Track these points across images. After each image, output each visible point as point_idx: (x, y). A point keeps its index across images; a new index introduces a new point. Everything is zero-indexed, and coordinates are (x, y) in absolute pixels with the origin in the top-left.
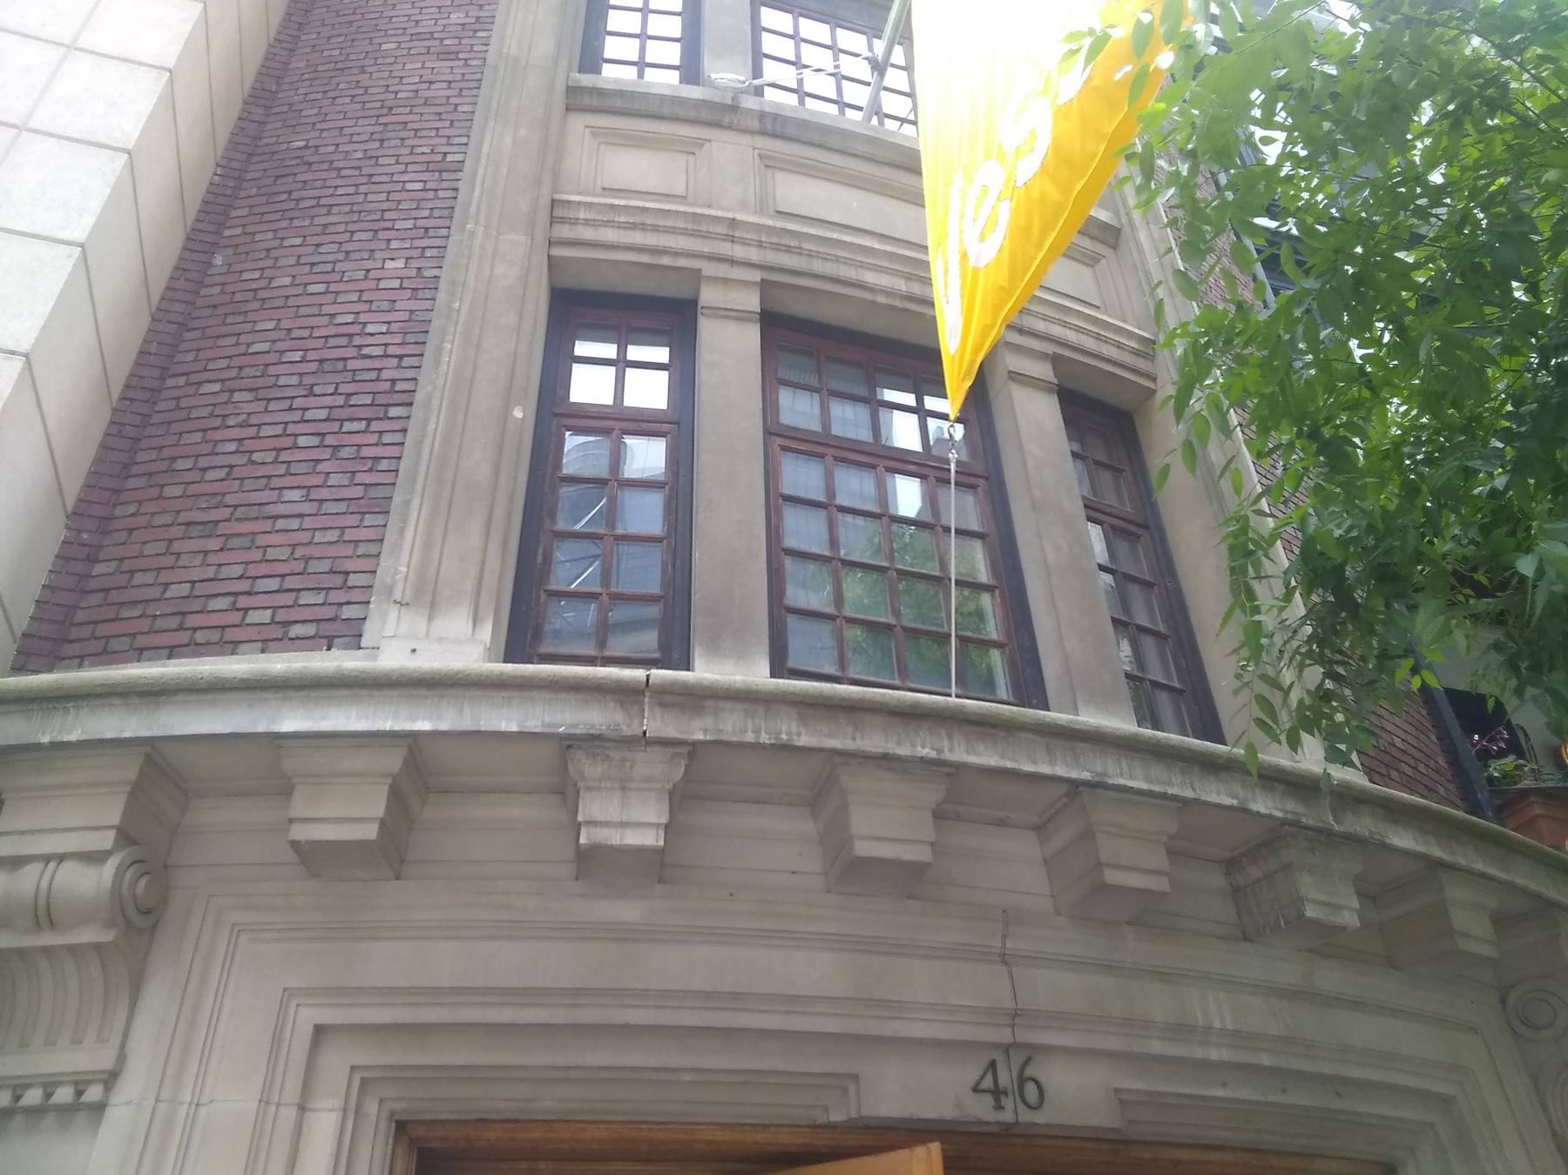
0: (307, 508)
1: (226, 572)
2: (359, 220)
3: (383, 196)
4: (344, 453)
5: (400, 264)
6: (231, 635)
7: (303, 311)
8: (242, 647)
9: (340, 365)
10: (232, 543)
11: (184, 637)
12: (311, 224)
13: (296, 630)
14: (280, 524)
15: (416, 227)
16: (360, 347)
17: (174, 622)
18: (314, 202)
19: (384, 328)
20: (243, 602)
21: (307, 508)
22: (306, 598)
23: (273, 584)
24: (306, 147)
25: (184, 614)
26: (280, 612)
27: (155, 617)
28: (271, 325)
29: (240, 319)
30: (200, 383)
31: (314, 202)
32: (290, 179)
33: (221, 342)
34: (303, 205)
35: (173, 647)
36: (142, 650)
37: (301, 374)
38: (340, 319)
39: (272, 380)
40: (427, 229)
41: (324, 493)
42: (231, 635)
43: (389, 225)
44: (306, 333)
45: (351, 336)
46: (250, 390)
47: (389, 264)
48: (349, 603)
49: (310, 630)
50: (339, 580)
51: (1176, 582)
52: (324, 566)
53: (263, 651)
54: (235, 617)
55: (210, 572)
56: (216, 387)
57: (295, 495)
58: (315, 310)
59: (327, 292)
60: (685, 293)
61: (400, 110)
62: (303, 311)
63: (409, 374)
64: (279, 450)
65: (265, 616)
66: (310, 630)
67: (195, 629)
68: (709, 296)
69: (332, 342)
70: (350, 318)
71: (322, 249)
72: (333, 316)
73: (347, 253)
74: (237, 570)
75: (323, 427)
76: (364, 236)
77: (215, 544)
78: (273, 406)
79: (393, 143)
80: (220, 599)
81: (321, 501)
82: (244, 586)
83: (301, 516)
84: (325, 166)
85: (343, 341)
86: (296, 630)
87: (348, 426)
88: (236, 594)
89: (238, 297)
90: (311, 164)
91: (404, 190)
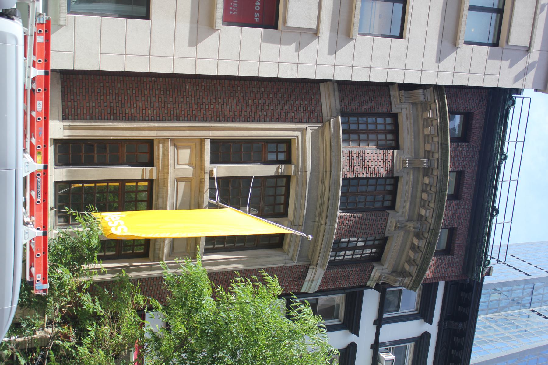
0: (91, 106)
4: (103, 111)
7: (137, 98)
13: (67, 110)
14: (88, 103)
17: (69, 91)
20: (72, 101)
22: (73, 110)
45: (131, 107)
54: (69, 100)
55: (78, 94)
57: (94, 104)
58: (138, 99)
62: (137, 98)
63: (121, 119)
66: (67, 112)
74: (79, 98)
77: (84, 94)
82: (75, 100)
86: (67, 110)
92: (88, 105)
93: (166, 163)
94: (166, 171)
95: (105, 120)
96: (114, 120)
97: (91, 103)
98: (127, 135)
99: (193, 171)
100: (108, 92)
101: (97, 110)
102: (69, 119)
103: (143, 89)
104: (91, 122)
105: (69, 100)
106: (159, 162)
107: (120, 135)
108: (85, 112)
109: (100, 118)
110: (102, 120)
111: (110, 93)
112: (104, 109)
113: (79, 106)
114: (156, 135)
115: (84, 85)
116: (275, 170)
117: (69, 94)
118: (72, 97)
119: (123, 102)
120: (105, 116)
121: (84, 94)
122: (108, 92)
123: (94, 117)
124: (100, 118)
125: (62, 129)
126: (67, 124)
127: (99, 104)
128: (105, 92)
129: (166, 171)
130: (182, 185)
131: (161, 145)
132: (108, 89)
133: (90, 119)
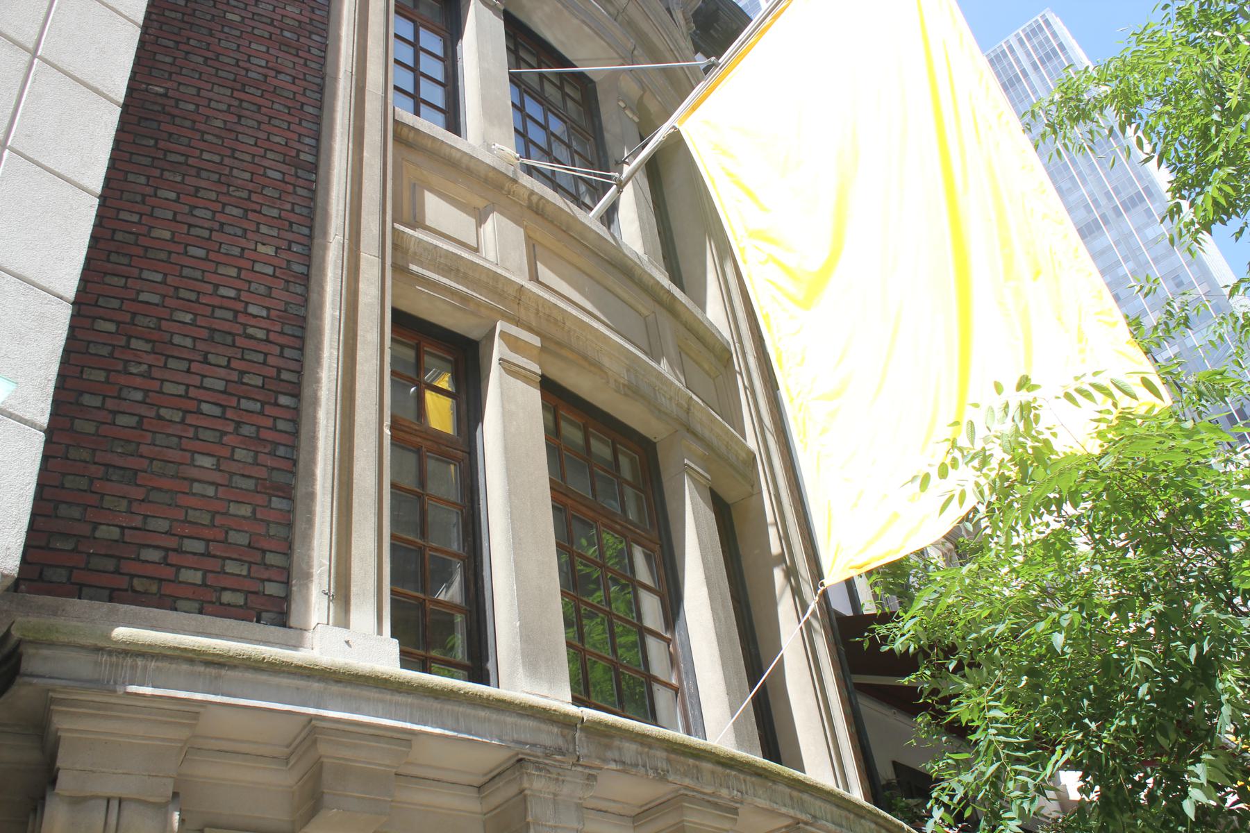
0: (217, 477)
1: (153, 524)
2: (228, 194)
3: (247, 176)
4: (247, 430)
5: (270, 251)
6: (168, 589)
7: (186, 272)
8: (180, 604)
9: (229, 340)
10: (155, 496)
11: (123, 582)
12: (182, 182)
13: (227, 597)
14: (197, 487)
15: (280, 218)
16: (245, 326)
17: (110, 565)
18: (182, 159)
19: (264, 313)
20: (174, 558)
21: (217, 477)
22: (231, 567)
23: (199, 547)
24: (165, 95)
25: (119, 558)
26: (210, 575)
27: (89, 555)
28: (159, 278)
29: (125, 260)
30: (94, 318)
31: (182, 159)
32: (155, 125)
33: (108, 279)
34: (172, 157)
35: (113, 590)
36: (81, 586)
37: (195, 339)
38: (222, 291)
39: (167, 337)
40: (291, 223)
41: (234, 467)
42: (168, 589)
43: (257, 207)
44: (193, 296)
45: (236, 312)
46: (148, 341)
47: (261, 248)
48: (269, 580)
49: (239, 599)
50: (257, 557)
51: (757, 649)
52: (243, 539)
53: (200, 612)
55: (138, 522)
56: (111, 327)
57: (207, 462)
58: (198, 274)
59: (206, 259)
60: (474, 335)
61: (252, 90)
62: (186, 272)
63: (293, 365)
64: (186, 412)
65: (197, 577)
66: (239, 599)
67: (132, 576)
68: (499, 349)
69: (218, 313)
70: (232, 293)
71: (196, 212)
72: (217, 286)
73: (222, 224)
74: (163, 525)
75: (223, 399)
76: (235, 211)
77: (138, 493)
78: (172, 363)
79: (251, 123)
80: (151, 550)
81: (232, 474)
82: (172, 543)
83: (217, 485)
84: (188, 124)
85: (229, 315)
86: (227, 597)
87: (245, 404)
88: (166, 549)
89: (119, 236)
90: (173, 116)
91: (264, 175)
92: (210, 491)
93: (484, 278)
94: (512, 291)
95: (296, 434)
96: (297, 395)
97: (194, 473)
98: (375, 362)
99: (502, 213)
100: (138, 381)
101: (240, 454)
102: (287, 598)
103: (142, 241)
104: (311, 496)
105: (168, 573)
106: (479, 304)
107: (374, 388)
108: (245, 511)
109: (281, 451)
110: (294, 447)
111: (147, 376)
112: (238, 424)
113: (207, 533)
114: (377, 261)
115: (83, 483)
116: (488, 13)
117: (127, 567)
118: (155, 555)
119: (205, 334)
120: (274, 428)
121: (138, 493)
122: (138, 381)
123: (279, 478)
124: (281, 451)
125: (342, 633)
126: (316, 604)
127: (204, 435)
128: (139, 396)
129: (512, 291)
130: (545, 273)
131: (413, 267)
132: (123, 380)
133: (290, 498)
